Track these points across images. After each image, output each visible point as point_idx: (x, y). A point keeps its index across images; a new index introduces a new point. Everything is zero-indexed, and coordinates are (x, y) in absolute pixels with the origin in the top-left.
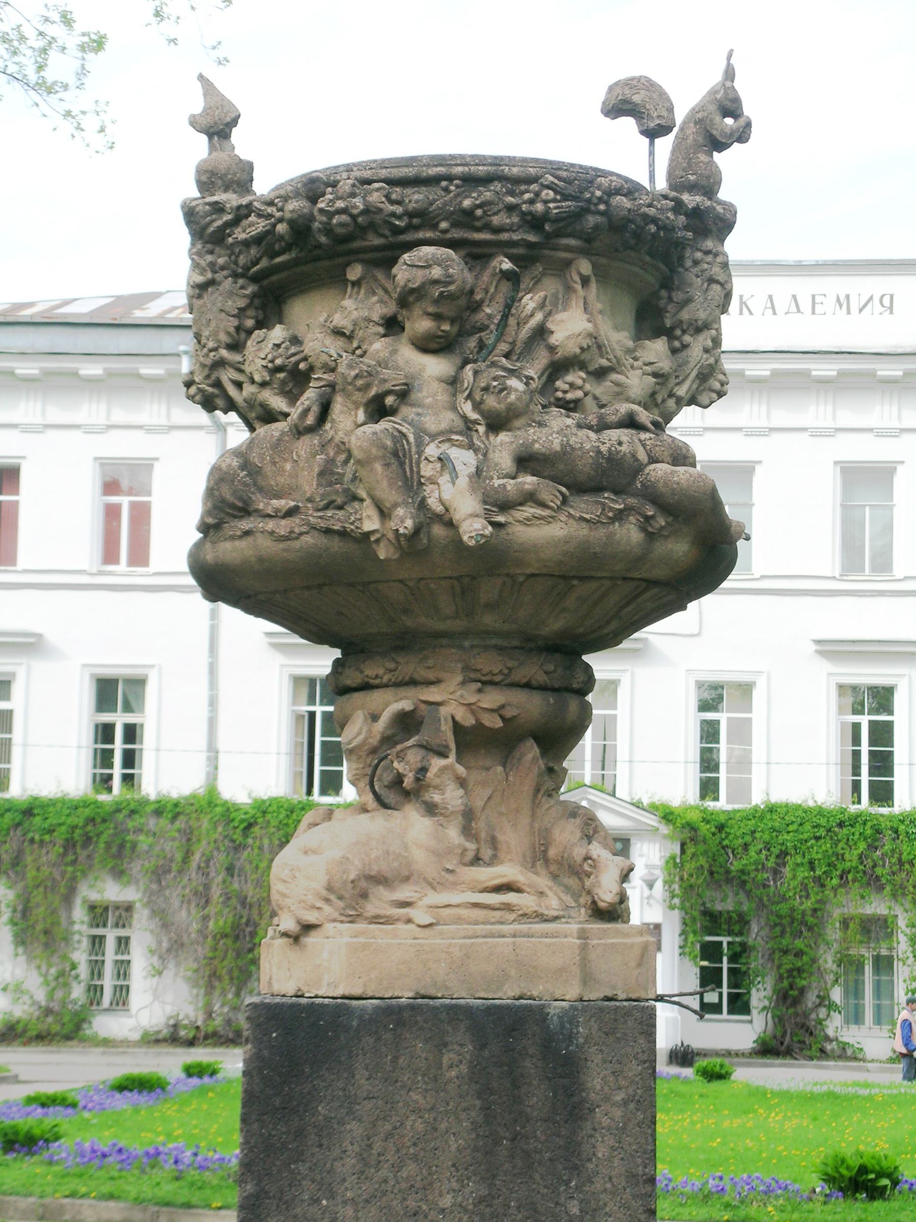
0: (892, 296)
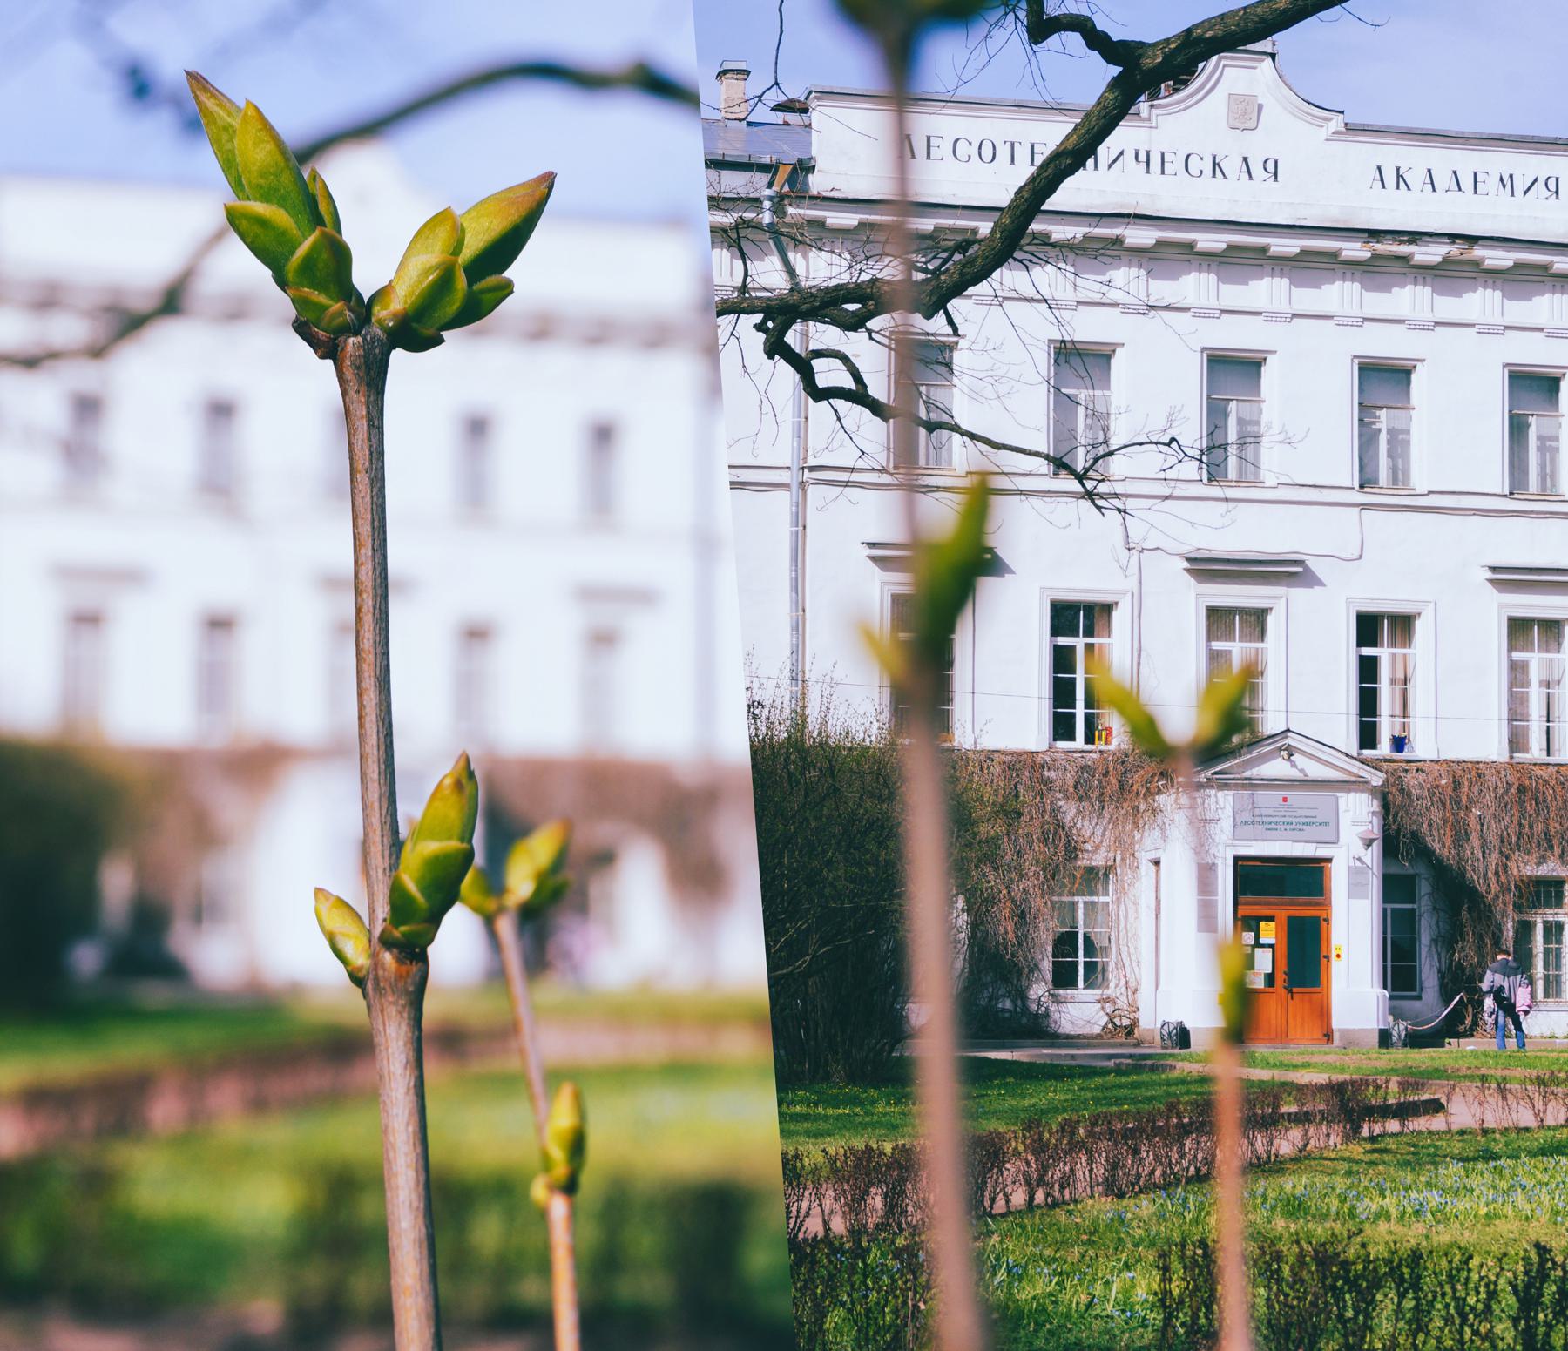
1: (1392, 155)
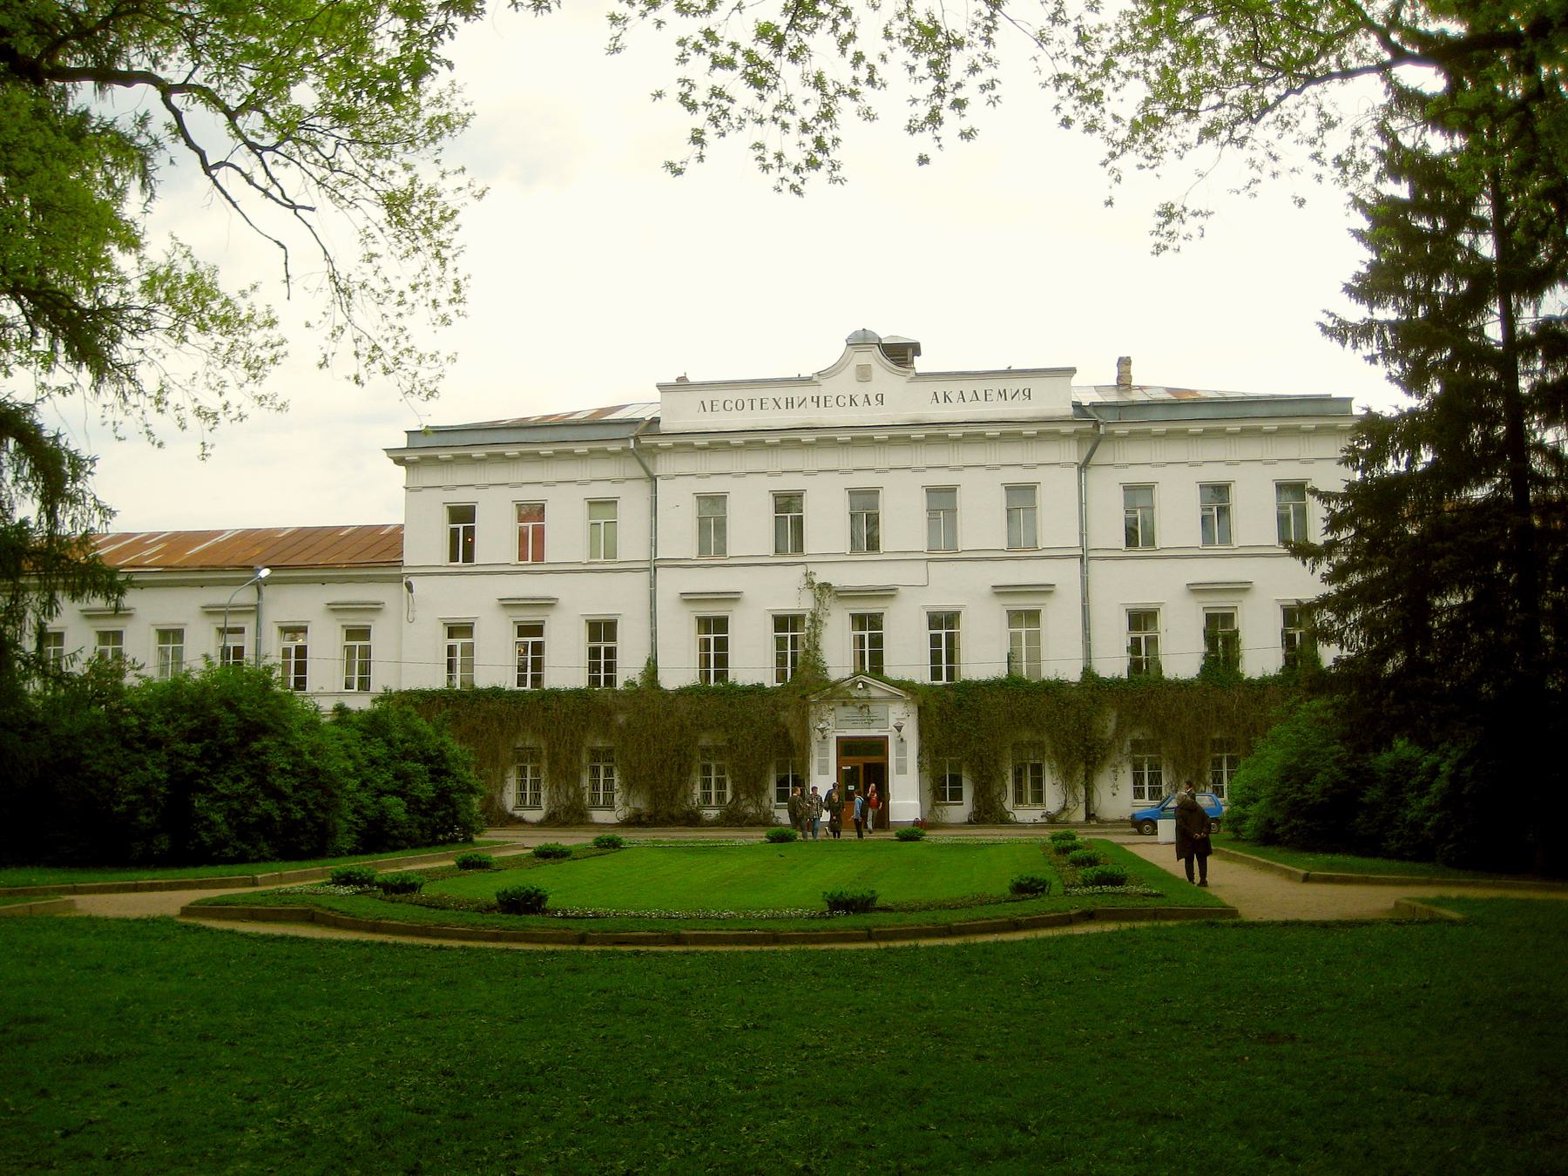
1: (941, 387)
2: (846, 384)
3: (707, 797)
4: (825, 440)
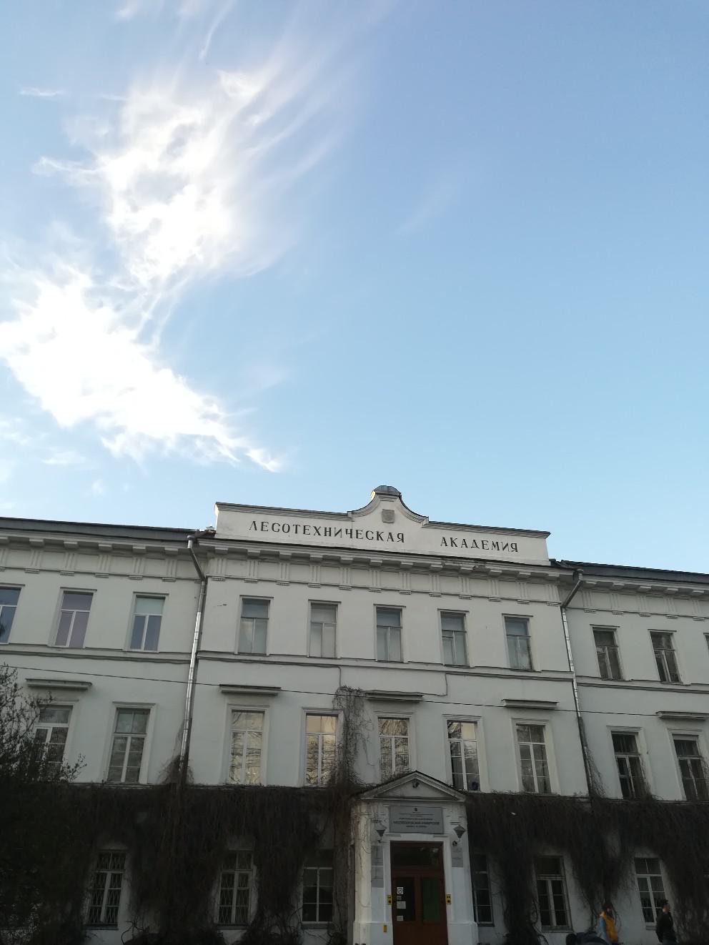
0: (516, 544)
2: (373, 522)
3: (225, 913)
4: (362, 562)
